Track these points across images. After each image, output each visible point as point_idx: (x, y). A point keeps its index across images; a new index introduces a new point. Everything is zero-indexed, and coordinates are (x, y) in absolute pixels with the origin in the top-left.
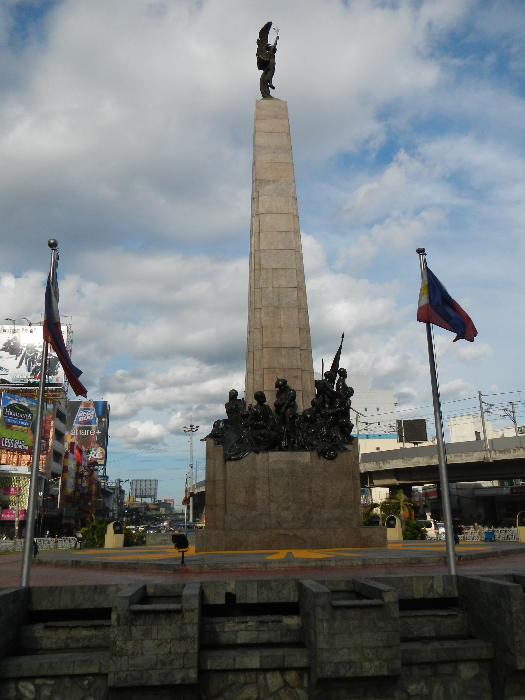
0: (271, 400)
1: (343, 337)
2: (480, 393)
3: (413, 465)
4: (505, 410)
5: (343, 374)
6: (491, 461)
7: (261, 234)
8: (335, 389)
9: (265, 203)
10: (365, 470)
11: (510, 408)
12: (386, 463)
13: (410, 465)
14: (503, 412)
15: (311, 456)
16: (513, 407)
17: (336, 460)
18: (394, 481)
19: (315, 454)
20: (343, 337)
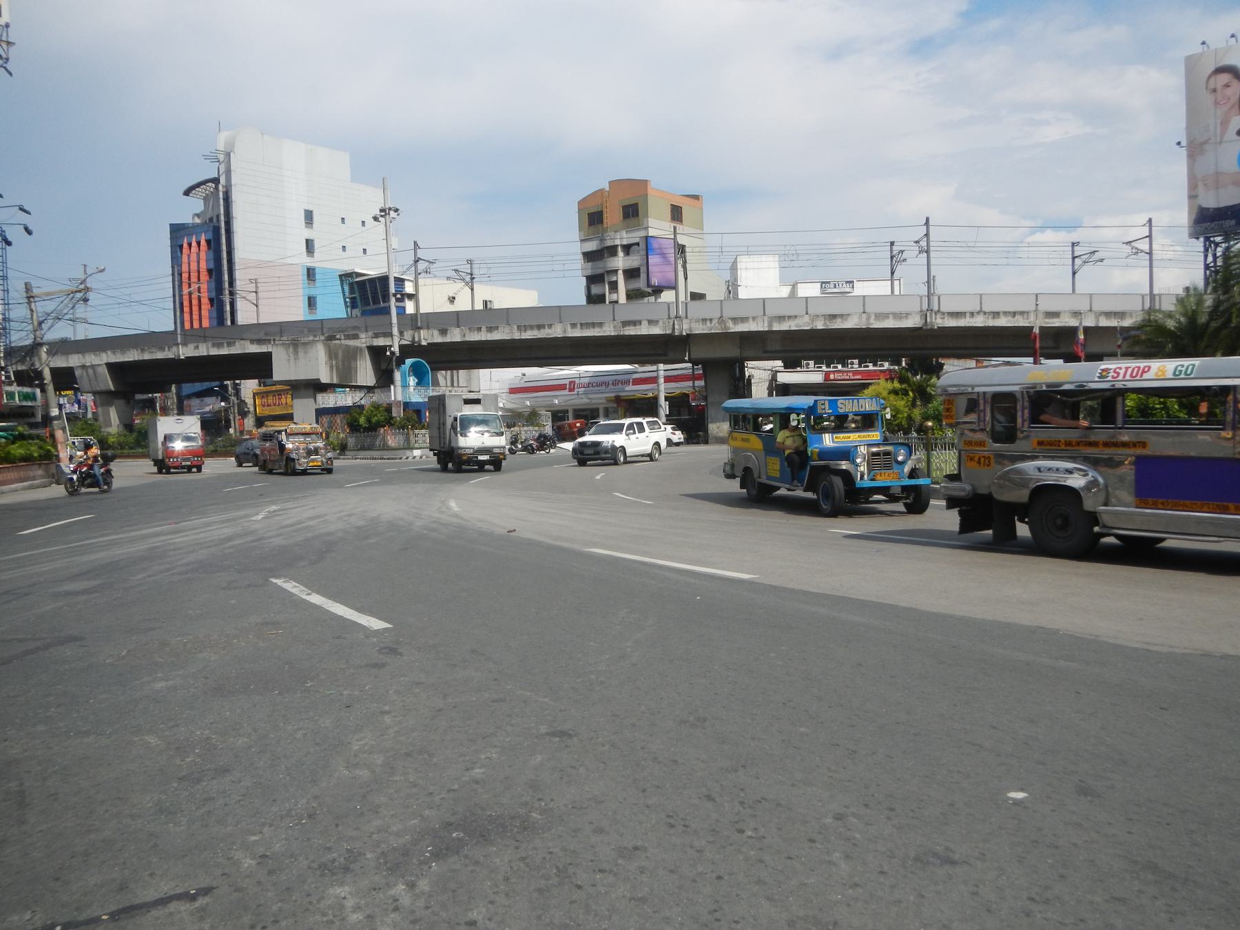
3: (796, 327)
6: (936, 327)
10: (690, 331)
12: (739, 322)
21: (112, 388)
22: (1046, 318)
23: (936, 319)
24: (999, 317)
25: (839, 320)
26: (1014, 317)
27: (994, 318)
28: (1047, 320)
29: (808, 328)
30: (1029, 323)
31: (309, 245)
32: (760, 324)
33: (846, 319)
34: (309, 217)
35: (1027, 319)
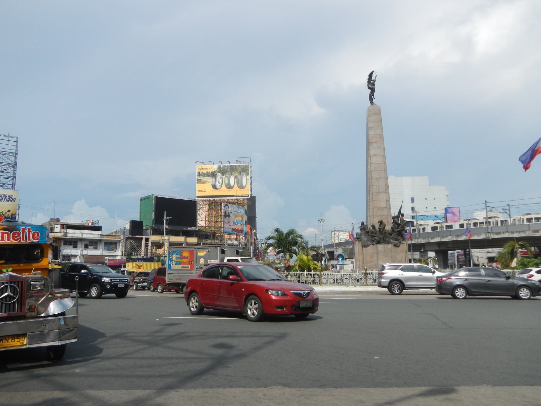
0: (377, 227)
1: (402, 202)
2: (486, 201)
4: (503, 209)
5: (403, 215)
6: (490, 238)
7: (372, 165)
8: (400, 222)
9: (372, 152)
11: (507, 208)
13: (446, 240)
14: (502, 211)
15: (391, 246)
16: (509, 208)
17: (400, 247)
18: (437, 248)
19: (392, 245)
20: (402, 202)
21: (329, 258)
22: (533, 233)
23: (490, 235)
24: (514, 234)
25: (460, 237)
26: (520, 233)
27: (512, 234)
28: (534, 234)
29: (451, 240)
30: (527, 235)
31: (413, 209)
32: (438, 240)
33: (462, 237)
34: (413, 200)
35: (525, 233)
